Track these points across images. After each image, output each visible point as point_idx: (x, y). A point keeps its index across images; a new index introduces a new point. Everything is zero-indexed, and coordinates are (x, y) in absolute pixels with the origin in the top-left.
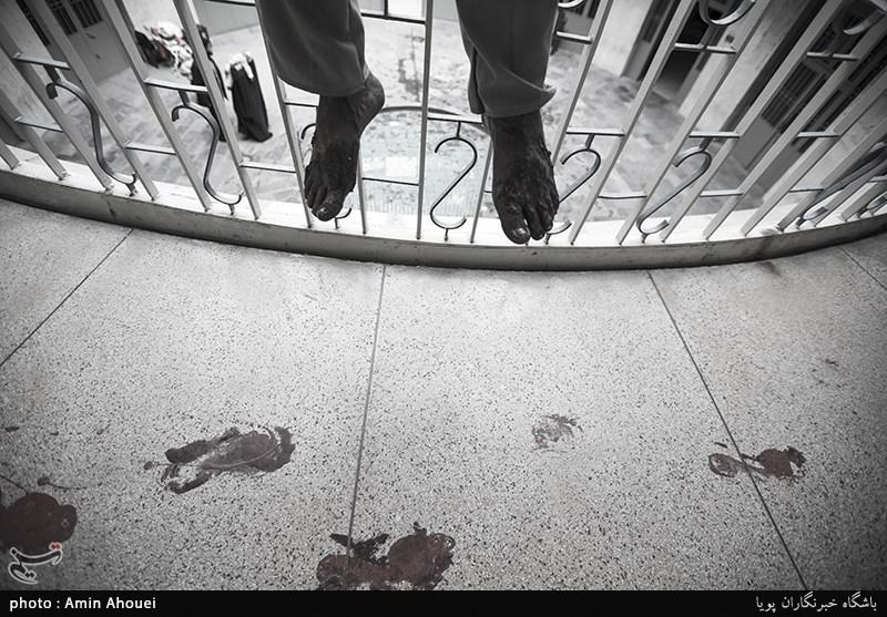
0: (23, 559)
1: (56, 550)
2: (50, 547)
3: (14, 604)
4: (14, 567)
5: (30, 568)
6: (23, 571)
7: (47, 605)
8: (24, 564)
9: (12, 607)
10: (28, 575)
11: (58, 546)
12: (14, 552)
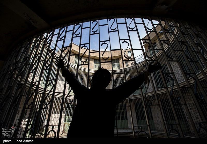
0: (5, 131)
1: (13, 128)
2: (12, 128)
3: (4, 141)
4: (3, 132)
5: (7, 133)
6: (5, 133)
8: (6, 132)
9: (4, 142)
10: (6, 134)
12: (3, 129)
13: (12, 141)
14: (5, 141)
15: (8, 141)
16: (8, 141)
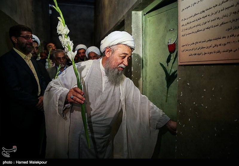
1: (15, 148)
2: (13, 147)
4: (3, 153)
6: (6, 154)
7: (10, 162)
9: (3, 163)
10: (7, 155)
11: (15, 147)
12: (3, 148)
13: (13, 163)
14: (4, 163)
15: (8, 163)
16: (8, 163)
